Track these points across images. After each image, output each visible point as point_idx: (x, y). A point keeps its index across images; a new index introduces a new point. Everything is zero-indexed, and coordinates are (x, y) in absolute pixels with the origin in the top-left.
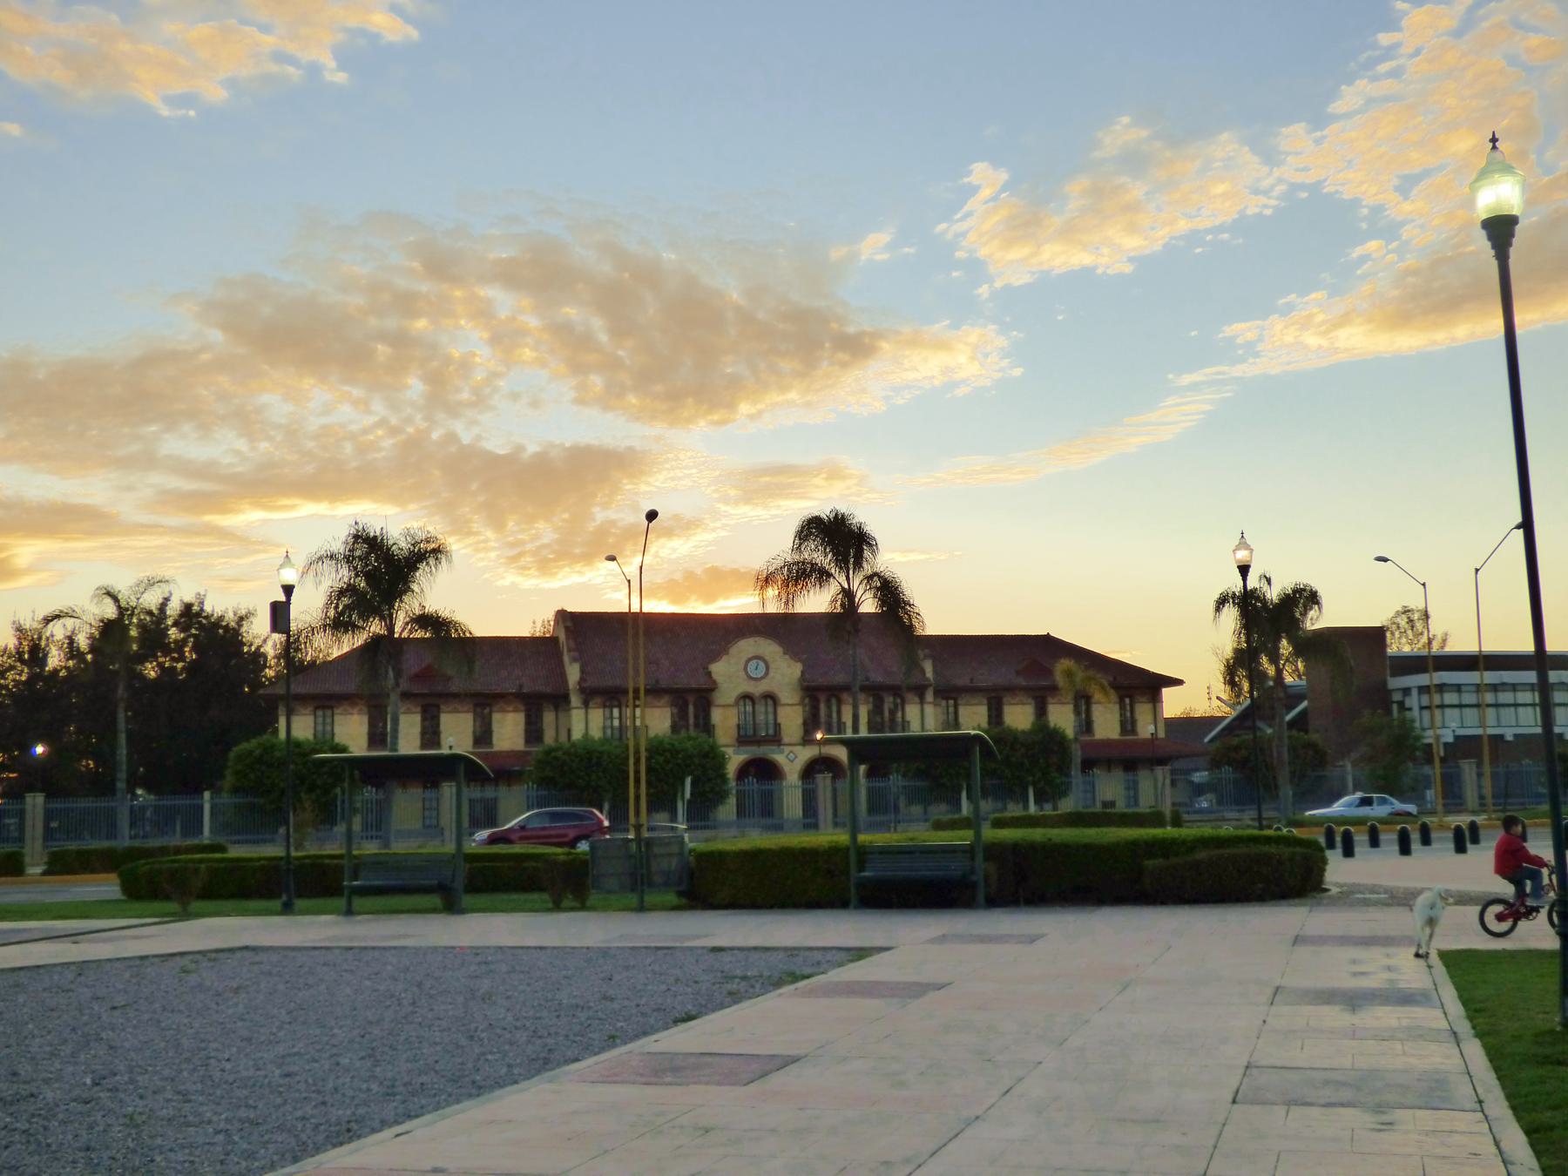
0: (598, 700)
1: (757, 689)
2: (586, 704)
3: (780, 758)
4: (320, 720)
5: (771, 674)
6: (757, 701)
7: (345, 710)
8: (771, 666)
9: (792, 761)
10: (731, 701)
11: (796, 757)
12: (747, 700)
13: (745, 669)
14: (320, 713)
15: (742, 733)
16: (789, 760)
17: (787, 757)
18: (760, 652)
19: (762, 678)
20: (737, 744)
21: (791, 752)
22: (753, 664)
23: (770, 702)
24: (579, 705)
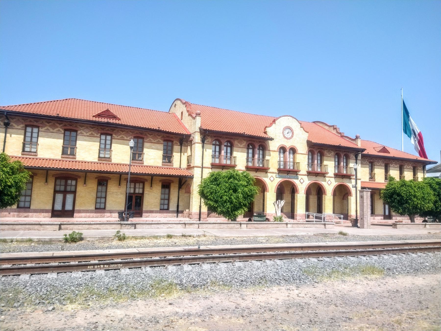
1: (288, 144)
2: (203, 141)
3: (296, 182)
4: (29, 134)
6: (288, 150)
7: (48, 129)
8: (294, 133)
9: (302, 183)
13: (283, 133)
14: (29, 129)
16: (301, 183)
17: (300, 181)
18: (290, 125)
19: (290, 138)
20: (277, 172)
22: (287, 131)
24: (200, 141)
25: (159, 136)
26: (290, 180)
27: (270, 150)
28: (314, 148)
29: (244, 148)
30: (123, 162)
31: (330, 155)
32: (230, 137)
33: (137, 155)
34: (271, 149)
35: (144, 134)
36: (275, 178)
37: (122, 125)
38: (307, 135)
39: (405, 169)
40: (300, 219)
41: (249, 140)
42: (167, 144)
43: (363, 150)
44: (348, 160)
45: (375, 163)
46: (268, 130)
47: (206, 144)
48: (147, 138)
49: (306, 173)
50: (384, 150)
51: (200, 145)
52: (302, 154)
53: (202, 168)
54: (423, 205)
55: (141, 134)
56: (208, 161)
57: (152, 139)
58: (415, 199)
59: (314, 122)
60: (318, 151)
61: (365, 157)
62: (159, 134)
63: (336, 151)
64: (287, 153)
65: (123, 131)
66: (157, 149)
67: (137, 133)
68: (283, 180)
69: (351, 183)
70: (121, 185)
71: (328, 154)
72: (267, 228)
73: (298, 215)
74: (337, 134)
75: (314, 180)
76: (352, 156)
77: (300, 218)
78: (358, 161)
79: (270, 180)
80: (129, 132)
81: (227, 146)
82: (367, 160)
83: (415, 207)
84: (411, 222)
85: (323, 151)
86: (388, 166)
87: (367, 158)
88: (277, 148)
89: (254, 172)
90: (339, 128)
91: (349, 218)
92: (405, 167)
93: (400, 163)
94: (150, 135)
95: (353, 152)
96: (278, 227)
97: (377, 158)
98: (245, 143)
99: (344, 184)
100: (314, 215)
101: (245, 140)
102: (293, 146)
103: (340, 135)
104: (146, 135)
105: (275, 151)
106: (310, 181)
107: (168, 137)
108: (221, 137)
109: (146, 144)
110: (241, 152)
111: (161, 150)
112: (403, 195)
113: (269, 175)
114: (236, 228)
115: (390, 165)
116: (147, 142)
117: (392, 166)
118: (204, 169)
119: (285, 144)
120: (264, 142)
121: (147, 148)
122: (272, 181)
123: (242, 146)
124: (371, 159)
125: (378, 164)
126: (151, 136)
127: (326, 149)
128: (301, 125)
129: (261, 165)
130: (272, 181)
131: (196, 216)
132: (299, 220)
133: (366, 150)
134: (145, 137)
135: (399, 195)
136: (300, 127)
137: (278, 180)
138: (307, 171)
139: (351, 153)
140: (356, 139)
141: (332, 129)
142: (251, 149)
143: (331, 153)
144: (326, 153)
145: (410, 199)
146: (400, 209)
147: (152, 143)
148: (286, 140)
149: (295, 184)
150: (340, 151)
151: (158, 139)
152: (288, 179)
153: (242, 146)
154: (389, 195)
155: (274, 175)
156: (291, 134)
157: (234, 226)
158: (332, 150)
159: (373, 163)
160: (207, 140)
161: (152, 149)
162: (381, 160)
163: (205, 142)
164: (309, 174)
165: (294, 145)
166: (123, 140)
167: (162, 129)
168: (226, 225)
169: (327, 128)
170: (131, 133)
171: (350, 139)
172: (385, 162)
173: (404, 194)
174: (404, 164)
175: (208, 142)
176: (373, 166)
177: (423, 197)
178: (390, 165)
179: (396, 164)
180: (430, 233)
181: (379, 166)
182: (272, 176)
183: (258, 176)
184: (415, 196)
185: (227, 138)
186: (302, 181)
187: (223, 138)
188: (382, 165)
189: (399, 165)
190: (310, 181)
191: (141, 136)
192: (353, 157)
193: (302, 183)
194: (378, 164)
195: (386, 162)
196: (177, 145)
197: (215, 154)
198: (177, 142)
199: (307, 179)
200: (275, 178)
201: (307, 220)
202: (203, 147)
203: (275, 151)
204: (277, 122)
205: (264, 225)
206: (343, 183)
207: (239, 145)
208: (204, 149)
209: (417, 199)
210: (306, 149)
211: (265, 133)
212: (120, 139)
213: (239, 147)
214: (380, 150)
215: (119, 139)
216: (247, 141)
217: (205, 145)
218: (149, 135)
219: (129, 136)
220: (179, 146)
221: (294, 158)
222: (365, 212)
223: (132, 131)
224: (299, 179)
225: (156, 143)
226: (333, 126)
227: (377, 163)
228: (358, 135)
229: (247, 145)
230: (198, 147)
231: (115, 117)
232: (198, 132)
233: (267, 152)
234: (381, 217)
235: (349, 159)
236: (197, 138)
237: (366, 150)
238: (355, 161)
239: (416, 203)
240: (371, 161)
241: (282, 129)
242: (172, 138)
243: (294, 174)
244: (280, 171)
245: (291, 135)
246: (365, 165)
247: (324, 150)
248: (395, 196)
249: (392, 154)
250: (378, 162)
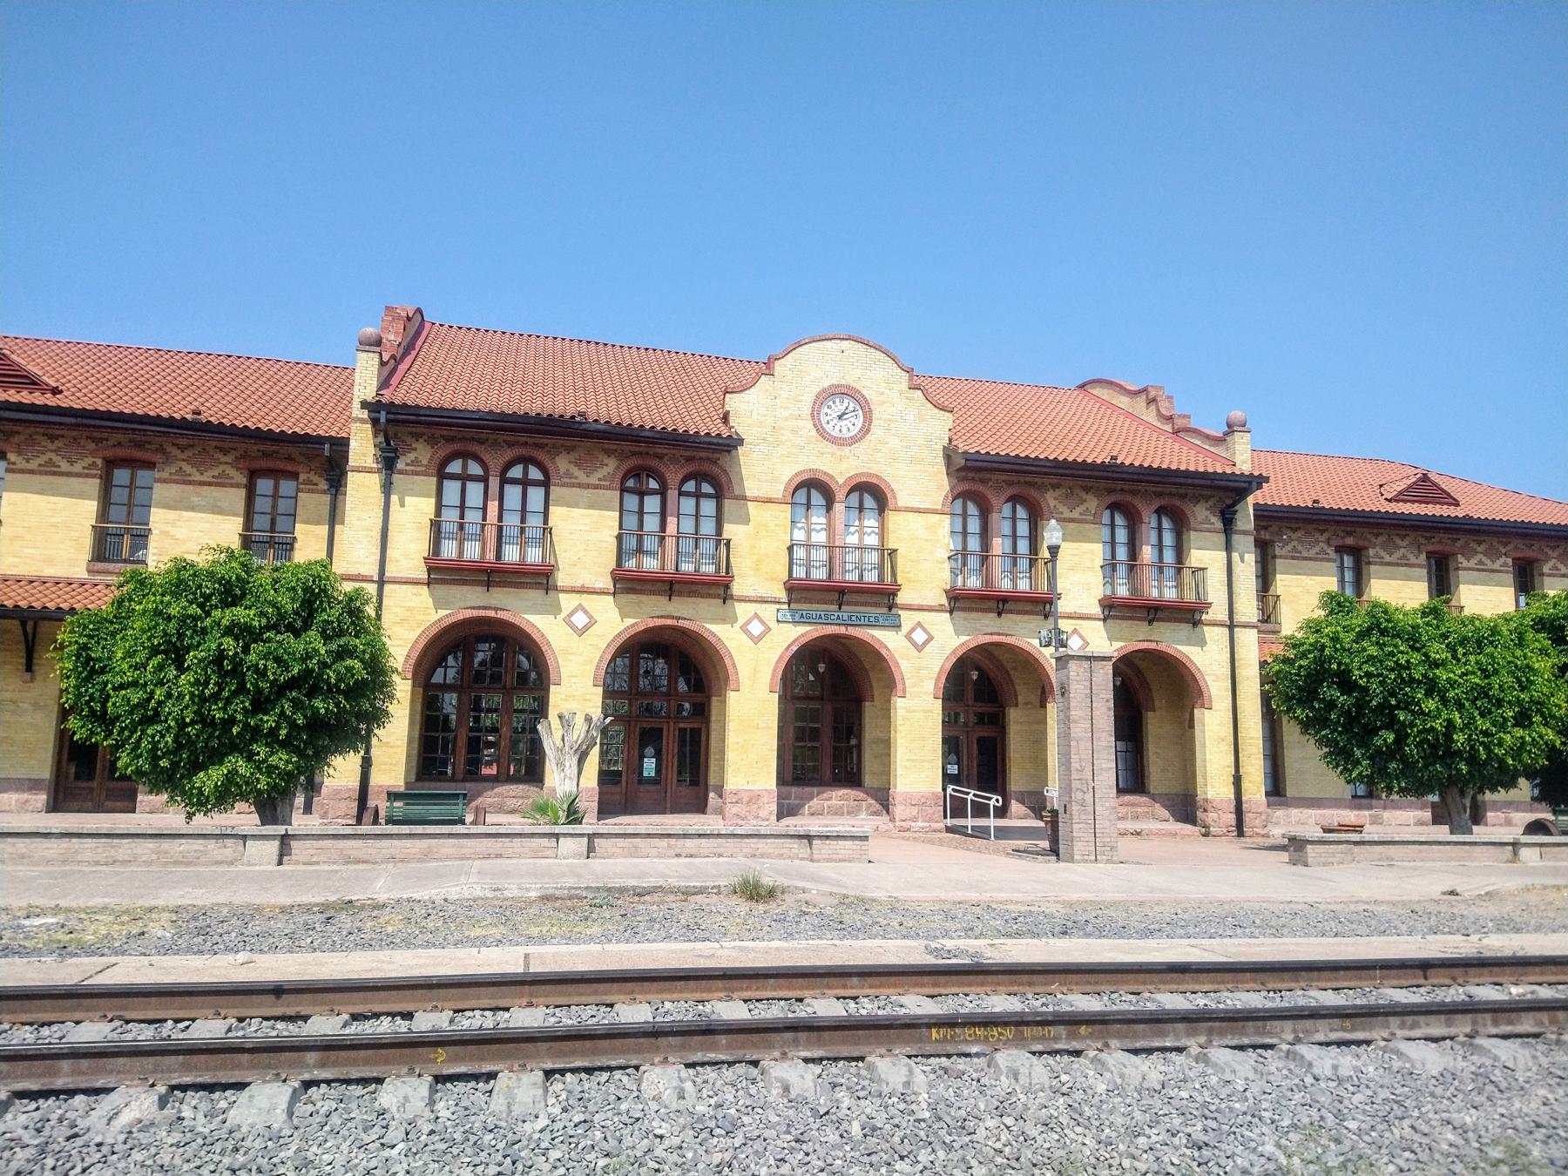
0: (423, 453)
1: (841, 468)
2: (388, 463)
3: (889, 641)
5: (877, 431)
6: (840, 495)
8: (876, 414)
9: (920, 648)
10: (778, 491)
11: (930, 638)
12: (813, 492)
15: (800, 573)
16: (914, 644)
17: (908, 637)
18: (851, 378)
19: (855, 440)
20: (783, 596)
21: (919, 624)
22: (839, 406)
23: (869, 502)
24: (370, 462)
25: (225, 451)
26: (852, 631)
27: (744, 498)
28: (983, 481)
29: (606, 488)
30: (49, 571)
31: (1075, 514)
32: (530, 441)
33: (127, 540)
34: (748, 494)
35: (153, 447)
36: (773, 624)
37: (70, 412)
38: (946, 420)
39: (1547, 580)
40: (915, 819)
41: (634, 454)
42: (276, 487)
43: (1258, 481)
44: (1185, 537)
45: (1371, 552)
46: (734, 403)
47: (401, 472)
48: (169, 459)
49: (944, 601)
50: (1425, 488)
51: (375, 480)
52: (918, 511)
53: (381, 582)
54: (1486, 733)
55: (139, 445)
56: (410, 553)
57: (188, 468)
58: (1431, 705)
59: (1082, 386)
60: (1004, 497)
61: (1310, 527)
62: (226, 445)
63: (1111, 491)
64: (839, 507)
65: (53, 438)
66: (216, 510)
67: (120, 444)
68: (815, 635)
69: (1202, 643)
70: (35, 668)
71: (1062, 508)
72: (425, 857)
73: (898, 799)
74: (1159, 425)
75: (986, 629)
76: (1202, 514)
77: (914, 811)
78: (1236, 538)
79: (747, 632)
80: (82, 442)
81: (525, 483)
82: (1326, 536)
83: (1440, 748)
84: (1452, 833)
85: (1036, 494)
86: (1452, 565)
87: (1322, 532)
88: (782, 487)
89: (663, 600)
90: (1170, 398)
91: (1199, 814)
92: (1546, 569)
93: (1517, 548)
94: (183, 449)
95: (1207, 498)
96: (499, 856)
97: (1377, 525)
98: (610, 466)
99: (1162, 647)
100: (970, 797)
101: (609, 453)
102: (870, 475)
103: (1168, 428)
104: (161, 450)
105: (769, 501)
106: (964, 638)
107: (265, 455)
108: (481, 442)
109: (160, 491)
110: (590, 506)
111: (235, 515)
112: (1362, 682)
113: (743, 610)
114: (218, 863)
115: (1460, 558)
116: (165, 481)
117: (1473, 563)
118: (388, 588)
119: (824, 469)
120: (715, 462)
121: (167, 506)
122: (756, 640)
123: (593, 480)
124: (1349, 534)
125: (1387, 559)
126: (188, 453)
127: (1055, 487)
128: (911, 379)
129: (708, 569)
130: (756, 640)
131: (343, 804)
132: (906, 825)
133: (1267, 480)
134: (158, 458)
135: (1345, 682)
136: (905, 385)
137: (788, 636)
138: (946, 592)
139: (1197, 500)
140: (1226, 434)
141: (1139, 406)
142: (653, 492)
143: (1083, 501)
144: (1052, 503)
145: (1406, 705)
146: (1357, 763)
147: (190, 483)
148: (830, 448)
149: (884, 652)
150: (1133, 493)
151: (222, 467)
152: (842, 630)
153: (593, 480)
154: (1299, 688)
155: (768, 611)
156: (859, 422)
157: (205, 852)
158: (1087, 490)
159: (1364, 553)
160: (411, 456)
161: (192, 508)
162: (1403, 537)
163: (400, 465)
164: (959, 601)
165: (874, 469)
166: (55, 473)
167: (211, 415)
168: (150, 844)
169: (1123, 401)
170: (92, 446)
171: (1208, 437)
172: (1430, 548)
173: (1368, 675)
174: (1540, 556)
175: (415, 462)
176: (1364, 567)
177: (1484, 692)
178: (1460, 558)
179: (1493, 554)
180: (1452, 893)
181: (1397, 565)
182: (756, 616)
183: (678, 618)
184: (1432, 687)
185: (510, 445)
186: (919, 637)
187: (495, 443)
188: (1413, 560)
189: (1510, 561)
190: (964, 638)
191: (138, 454)
192: (1207, 521)
193: (920, 648)
194: (1387, 559)
195: (1437, 548)
196: (312, 491)
197: (462, 517)
198: (315, 479)
199: (950, 628)
200: (773, 624)
201: (949, 822)
202: (387, 488)
203: (769, 501)
204: (778, 366)
205: (408, 843)
206: (1153, 646)
207: (581, 477)
208: (394, 498)
209: (1444, 701)
210: (940, 488)
211: (725, 418)
212: (41, 473)
213: (580, 486)
214: (1400, 493)
215: (32, 472)
216: (622, 457)
217: (396, 477)
218: (175, 452)
219: (83, 456)
220: (324, 492)
221: (882, 532)
222: (1080, 771)
223: (96, 434)
224: (905, 629)
225: (209, 484)
226: (1145, 390)
227: (1382, 553)
228: (1237, 415)
229: (620, 475)
230: (362, 488)
231: (32, 382)
232: (362, 421)
233: (727, 503)
234: (1419, 813)
235: (1189, 529)
236: (363, 447)
237: (1267, 480)
238: (1222, 537)
239: (1438, 725)
240: (1350, 541)
241: (809, 398)
242: (290, 459)
243: (876, 605)
244: (800, 593)
245: (859, 426)
246: (1311, 563)
247: (1042, 488)
248: (1330, 692)
249: (1475, 505)
250: (1390, 547)
